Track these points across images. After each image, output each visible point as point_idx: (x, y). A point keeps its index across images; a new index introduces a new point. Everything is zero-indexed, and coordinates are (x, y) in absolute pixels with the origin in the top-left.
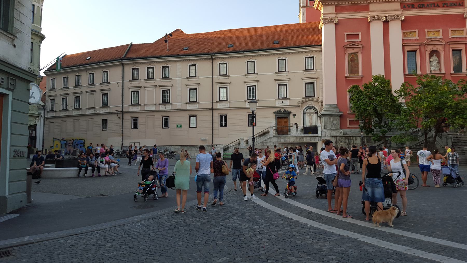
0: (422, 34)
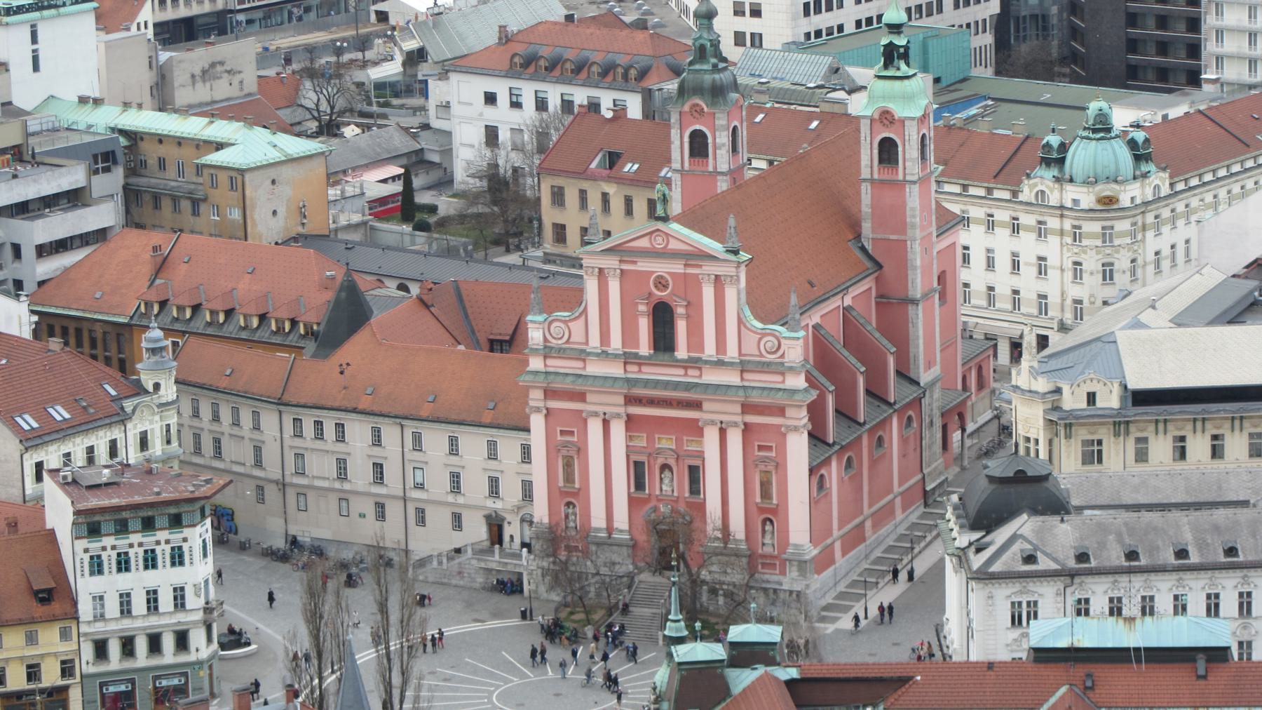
0: (650, 440)
